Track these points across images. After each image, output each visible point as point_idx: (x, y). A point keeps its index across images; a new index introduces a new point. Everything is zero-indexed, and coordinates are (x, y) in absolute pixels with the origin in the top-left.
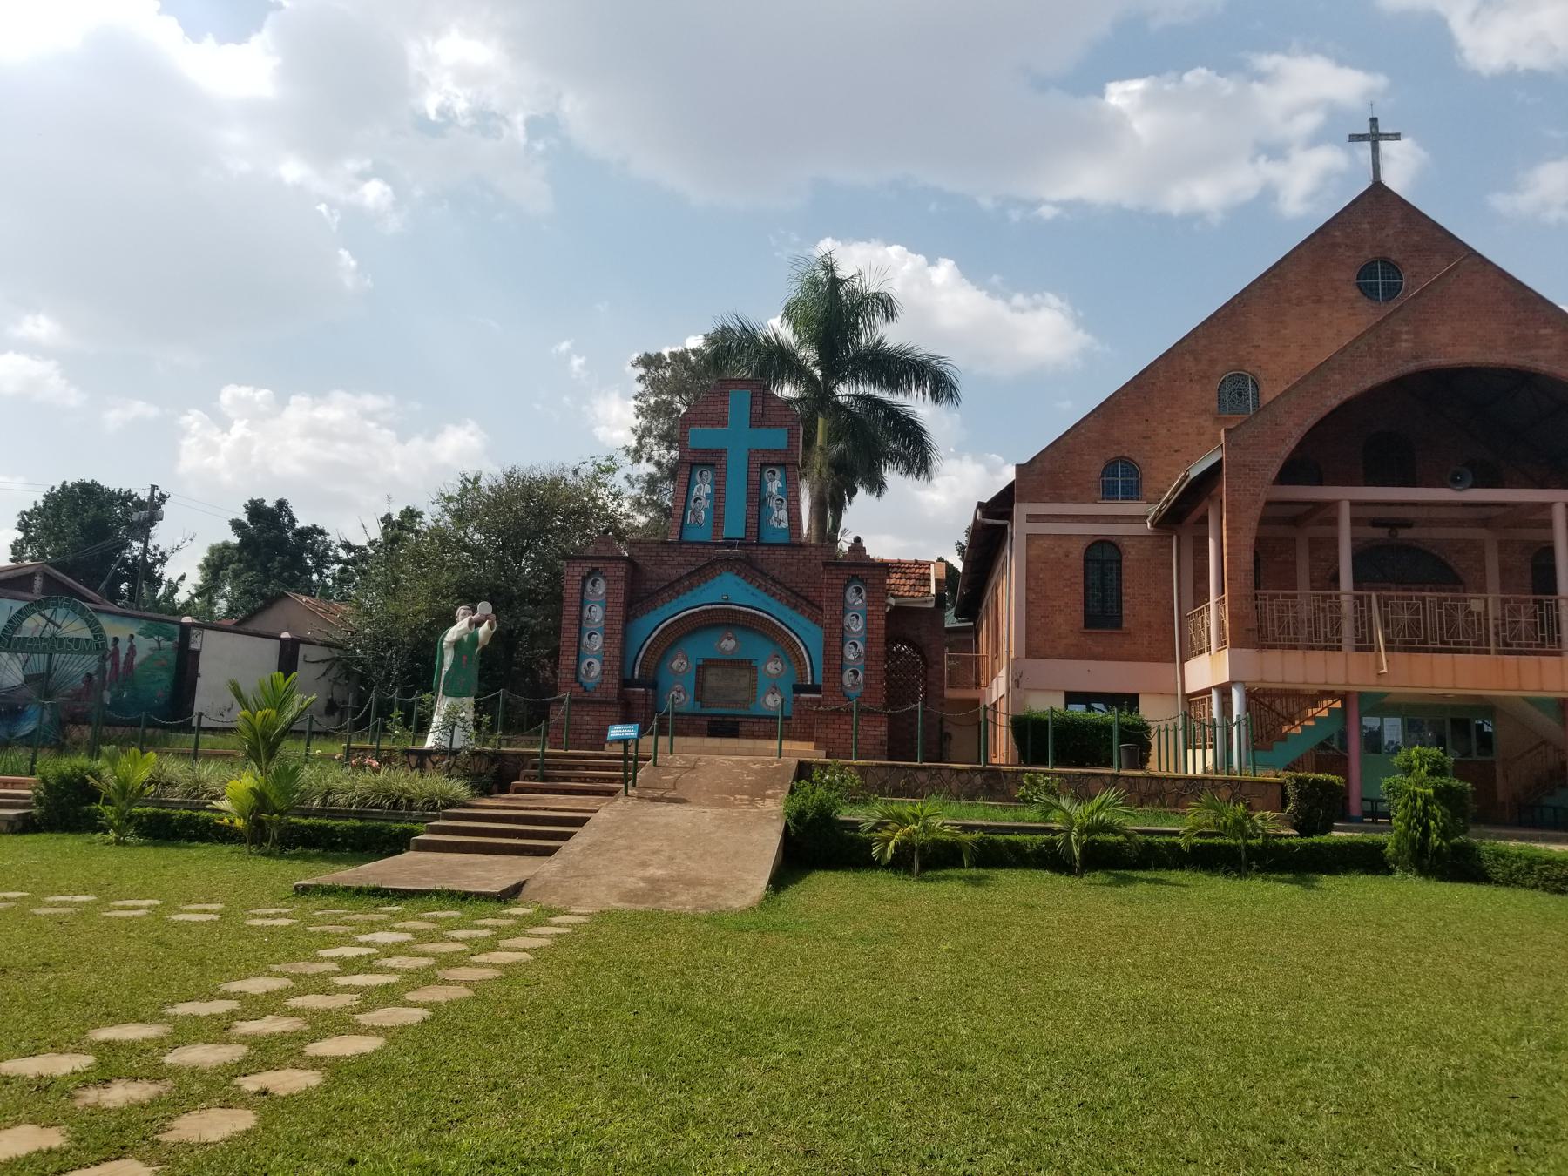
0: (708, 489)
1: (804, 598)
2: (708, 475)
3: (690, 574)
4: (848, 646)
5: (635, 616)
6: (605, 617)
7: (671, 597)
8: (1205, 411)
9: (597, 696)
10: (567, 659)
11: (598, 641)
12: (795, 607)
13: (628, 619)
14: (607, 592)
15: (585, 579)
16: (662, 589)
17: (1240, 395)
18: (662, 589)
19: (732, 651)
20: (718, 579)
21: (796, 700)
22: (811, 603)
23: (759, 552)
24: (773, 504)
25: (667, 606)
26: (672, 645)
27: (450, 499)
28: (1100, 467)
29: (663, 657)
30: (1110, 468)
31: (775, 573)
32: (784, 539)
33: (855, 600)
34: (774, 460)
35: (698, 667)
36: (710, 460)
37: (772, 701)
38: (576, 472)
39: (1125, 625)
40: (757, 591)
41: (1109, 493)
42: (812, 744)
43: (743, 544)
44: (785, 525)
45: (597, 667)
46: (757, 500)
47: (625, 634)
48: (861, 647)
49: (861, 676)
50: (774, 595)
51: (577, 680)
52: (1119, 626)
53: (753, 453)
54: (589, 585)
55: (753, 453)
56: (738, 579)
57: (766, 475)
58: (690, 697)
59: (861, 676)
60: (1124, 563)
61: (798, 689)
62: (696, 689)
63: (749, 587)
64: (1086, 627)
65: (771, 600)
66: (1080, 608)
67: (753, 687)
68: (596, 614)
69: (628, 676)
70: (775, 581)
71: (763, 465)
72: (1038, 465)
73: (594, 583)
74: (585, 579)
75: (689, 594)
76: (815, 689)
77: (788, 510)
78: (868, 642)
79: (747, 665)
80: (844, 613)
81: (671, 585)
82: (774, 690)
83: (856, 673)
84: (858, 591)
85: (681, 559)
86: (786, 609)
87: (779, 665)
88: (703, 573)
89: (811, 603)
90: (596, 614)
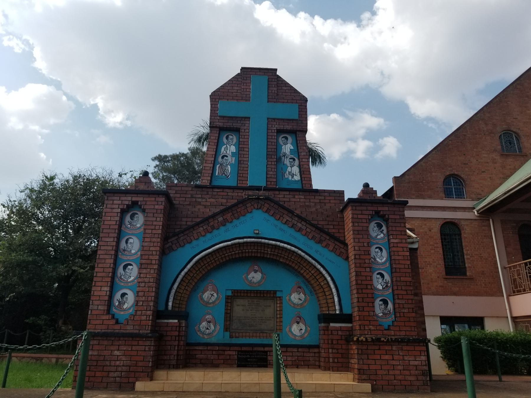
0: (233, 149)
1: (328, 234)
2: (234, 138)
3: (222, 212)
4: (375, 276)
5: (171, 249)
6: (142, 248)
7: (207, 231)
8: (495, 151)
9: (130, 329)
10: (100, 290)
11: (133, 272)
12: (320, 242)
13: (164, 252)
14: (145, 224)
15: (123, 212)
16: (198, 224)
17: (510, 143)
18: (198, 224)
19: (259, 282)
20: (249, 215)
21: (327, 329)
22: (332, 237)
23: (280, 197)
24: (287, 162)
25: (202, 239)
26: (203, 278)
27: (32, 190)
28: (442, 180)
29: (194, 289)
30: (447, 180)
31: (298, 212)
32: (299, 186)
33: (377, 234)
34: (288, 127)
35: (227, 297)
36: (236, 125)
37: (297, 330)
38: (120, 175)
39: (468, 274)
40: (285, 227)
41: (448, 195)
42: (350, 375)
43: (266, 189)
44: (297, 178)
45: (131, 298)
46: (274, 157)
47: (160, 265)
48: (387, 277)
49: (390, 306)
50: (300, 230)
51: (108, 311)
52: (465, 274)
53: (271, 121)
54: (128, 218)
55: (271, 121)
56: (266, 216)
57: (281, 140)
58: (220, 327)
59: (390, 306)
60: (463, 235)
61: (326, 318)
62: (226, 320)
63: (278, 223)
64: (447, 274)
65: (298, 235)
66: (442, 262)
67: (278, 316)
68: (134, 245)
69: (162, 308)
70: (301, 218)
71: (280, 132)
72: (407, 177)
73: (132, 217)
74: (123, 212)
75: (222, 229)
76: (347, 318)
77: (300, 166)
78: (393, 271)
79: (271, 296)
80: (369, 245)
81: (206, 220)
82: (299, 320)
83: (385, 302)
84: (380, 226)
85: (212, 200)
86: (312, 243)
87: (302, 296)
88: (234, 210)
89: (332, 237)
90: (134, 245)
